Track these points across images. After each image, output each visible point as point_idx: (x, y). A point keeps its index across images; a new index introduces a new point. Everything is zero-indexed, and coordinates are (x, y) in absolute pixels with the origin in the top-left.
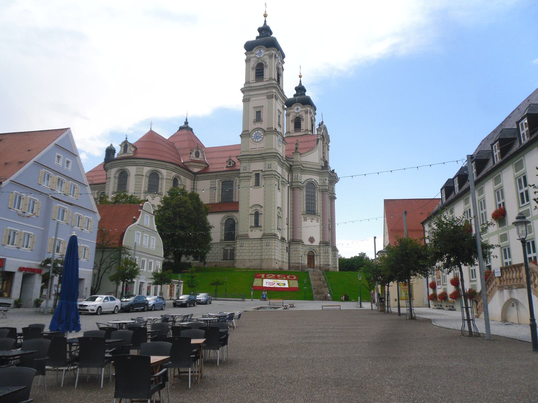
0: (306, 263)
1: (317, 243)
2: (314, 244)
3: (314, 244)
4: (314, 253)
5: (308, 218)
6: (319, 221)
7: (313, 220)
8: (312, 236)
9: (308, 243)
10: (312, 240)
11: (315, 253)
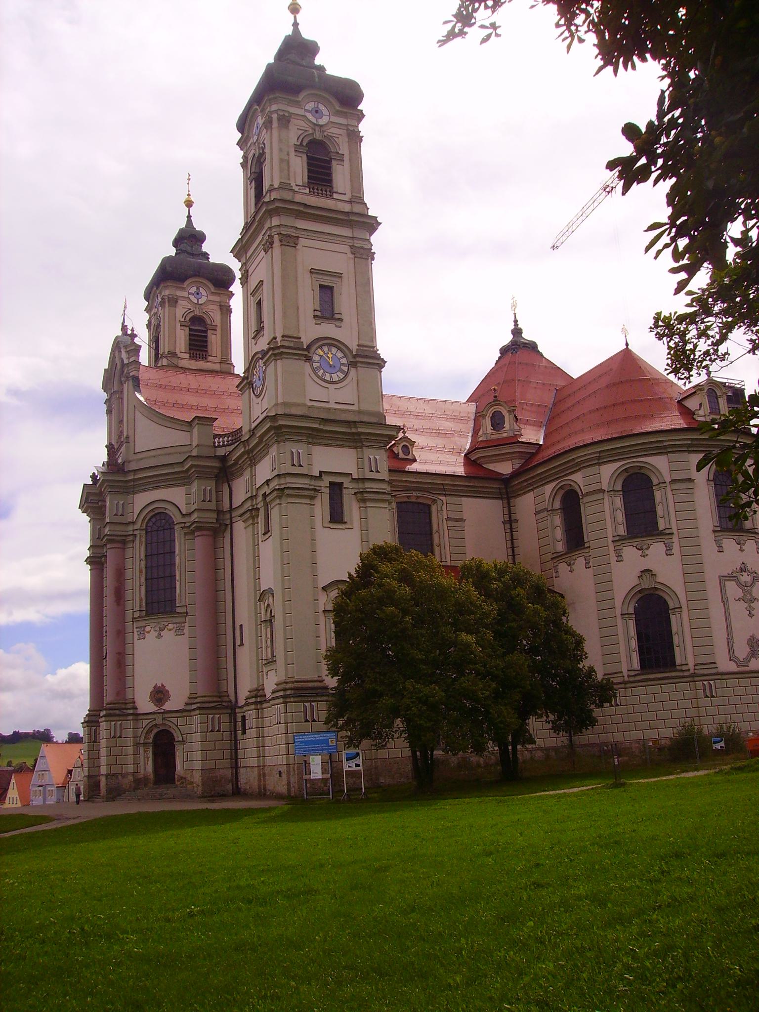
0: (149, 767)
1: (174, 703)
2: (168, 706)
3: (168, 706)
4: (173, 735)
5: (148, 628)
6: (186, 630)
7: (162, 630)
8: (159, 685)
9: (151, 707)
10: (159, 696)
11: (175, 735)
